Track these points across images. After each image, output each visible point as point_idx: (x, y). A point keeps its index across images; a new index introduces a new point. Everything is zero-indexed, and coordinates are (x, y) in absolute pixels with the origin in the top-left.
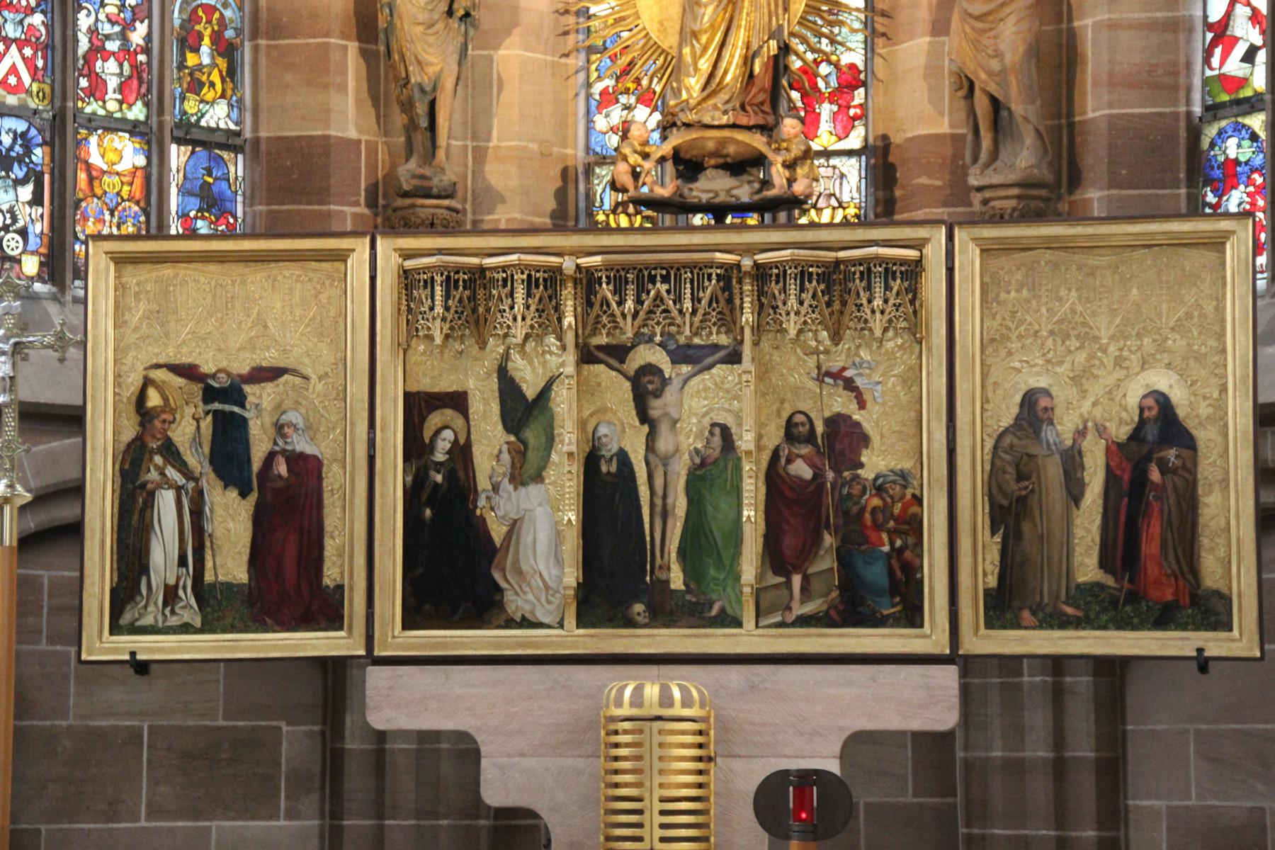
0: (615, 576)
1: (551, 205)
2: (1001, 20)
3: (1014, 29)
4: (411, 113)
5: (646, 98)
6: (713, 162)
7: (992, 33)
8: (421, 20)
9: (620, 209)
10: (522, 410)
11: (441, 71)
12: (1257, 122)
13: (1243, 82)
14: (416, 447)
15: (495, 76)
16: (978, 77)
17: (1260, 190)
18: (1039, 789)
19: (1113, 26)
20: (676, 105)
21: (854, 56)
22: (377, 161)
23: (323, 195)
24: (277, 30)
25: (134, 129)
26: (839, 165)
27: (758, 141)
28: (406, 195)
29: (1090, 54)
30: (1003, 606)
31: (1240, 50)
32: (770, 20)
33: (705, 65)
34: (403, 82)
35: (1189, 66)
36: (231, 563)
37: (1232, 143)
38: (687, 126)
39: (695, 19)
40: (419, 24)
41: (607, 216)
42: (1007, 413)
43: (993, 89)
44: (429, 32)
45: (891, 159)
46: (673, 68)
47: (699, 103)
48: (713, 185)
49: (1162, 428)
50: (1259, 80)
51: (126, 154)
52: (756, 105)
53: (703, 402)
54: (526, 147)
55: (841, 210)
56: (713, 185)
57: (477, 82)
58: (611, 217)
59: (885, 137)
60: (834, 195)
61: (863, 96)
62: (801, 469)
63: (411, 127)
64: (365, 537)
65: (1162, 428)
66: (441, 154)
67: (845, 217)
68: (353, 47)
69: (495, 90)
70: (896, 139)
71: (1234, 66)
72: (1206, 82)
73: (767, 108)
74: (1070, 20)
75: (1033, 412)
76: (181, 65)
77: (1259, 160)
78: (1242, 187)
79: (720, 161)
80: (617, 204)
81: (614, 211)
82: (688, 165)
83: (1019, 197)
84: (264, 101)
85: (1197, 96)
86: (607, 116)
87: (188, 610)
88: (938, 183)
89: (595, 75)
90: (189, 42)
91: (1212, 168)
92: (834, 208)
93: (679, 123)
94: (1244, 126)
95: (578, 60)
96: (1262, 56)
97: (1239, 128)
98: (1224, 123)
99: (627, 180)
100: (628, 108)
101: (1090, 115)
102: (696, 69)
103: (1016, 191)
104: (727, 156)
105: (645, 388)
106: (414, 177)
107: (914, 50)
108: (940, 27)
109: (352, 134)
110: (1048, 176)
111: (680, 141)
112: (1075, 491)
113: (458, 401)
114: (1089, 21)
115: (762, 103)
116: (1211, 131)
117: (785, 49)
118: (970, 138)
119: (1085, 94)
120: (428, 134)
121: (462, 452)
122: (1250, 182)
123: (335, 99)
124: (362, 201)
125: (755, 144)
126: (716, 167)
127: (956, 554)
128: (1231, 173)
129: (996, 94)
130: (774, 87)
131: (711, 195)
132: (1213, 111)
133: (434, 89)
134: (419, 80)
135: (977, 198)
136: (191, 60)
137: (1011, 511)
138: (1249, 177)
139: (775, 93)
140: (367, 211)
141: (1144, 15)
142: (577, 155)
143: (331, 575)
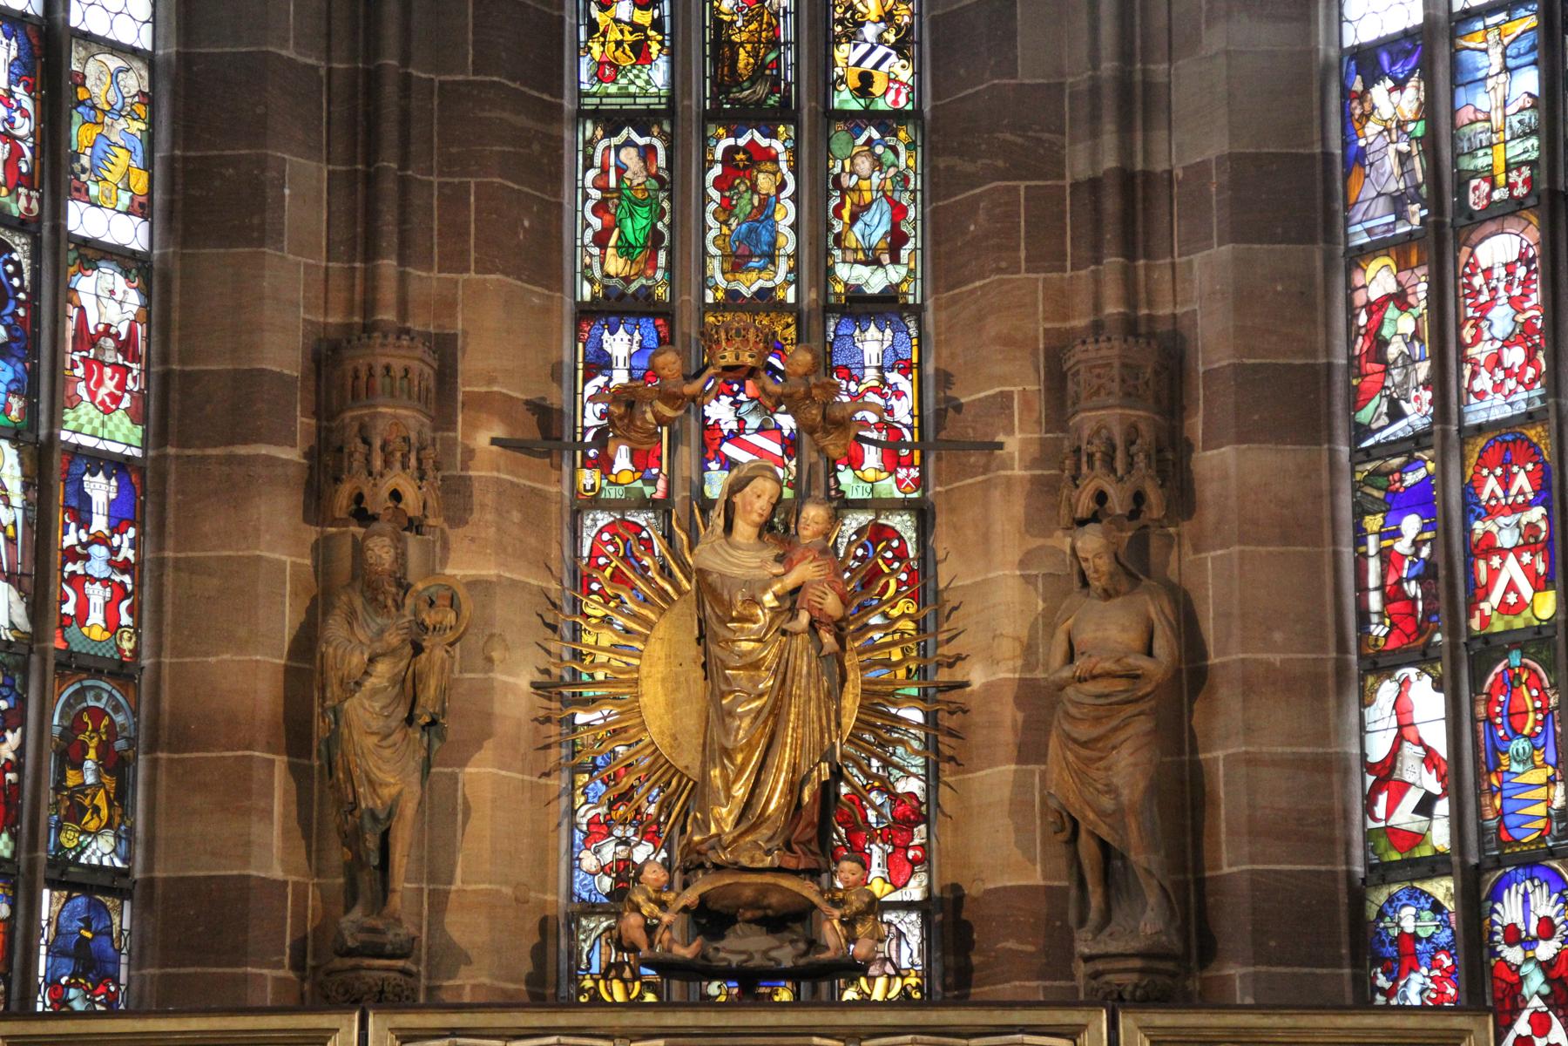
1: (527, 967)
2: (1114, 748)
3: (1132, 760)
4: (357, 849)
5: (649, 832)
6: (749, 915)
7: (1102, 764)
8: (374, 729)
9: (613, 973)
11: (400, 793)
12: (1441, 888)
13: (1418, 838)
15: (460, 801)
16: (1085, 817)
17: (1449, 974)
19: (1251, 761)
20: (702, 842)
21: (914, 786)
22: (306, 908)
23: (238, 955)
24: (183, 739)
26: (896, 921)
27: (808, 890)
28: (350, 953)
29: (1222, 794)
31: (1412, 798)
32: (822, 737)
33: (739, 791)
34: (347, 807)
35: (1346, 815)
37: (1408, 913)
38: (718, 867)
39: (727, 733)
40: (373, 733)
41: (596, 982)
43: (1104, 831)
44: (384, 744)
45: (964, 916)
46: (699, 793)
47: (735, 840)
48: (746, 944)
50: (1440, 836)
52: (803, 843)
54: (498, 891)
55: (898, 980)
56: (746, 944)
57: (443, 811)
58: (602, 983)
59: (956, 888)
60: (890, 959)
61: (924, 834)
63: (353, 869)
66: (395, 901)
67: (904, 988)
68: (281, 761)
69: (460, 817)
70: (972, 890)
71: (1405, 817)
72: (1368, 835)
73: (814, 847)
74: (1194, 750)
76: (60, 786)
77: (1444, 937)
78: (1424, 970)
79: (759, 913)
80: (610, 966)
81: (605, 975)
82: (710, 919)
83: (1141, 971)
84: (162, 831)
85: (1358, 852)
86: (597, 852)
88: (1030, 948)
89: (582, 799)
90: (71, 756)
91: (1383, 943)
92: (889, 977)
93: (708, 865)
94: (1423, 893)
95: (559, 782)
96: (1442, 807)
97: (1416, 895)
98: (1395, 888)
99: (639, 937)
100: (623, 841)
101: (1226, 870)
102: (729, 797)
103: (1137, 963)
104: (770, 907)
106: (362, 929)
107: (994, 778)
108: (1030, 750)
109: (277, 873)
110: (1177, 946)
111: (709, 887)
114: (1220, 754)
115: (810, 841)
116: (1380, 897)
117: (838, 774)
118: (1073, 893)
119: (1218, 844)
120: (378, 874)
122: (1434, 964)
123: (257, 829)
124: (287, 961)
125: (805, 893)
126: (749, 922)
128: (1407, 953)
129: (1108, 839)
130: (823, 825)
131: (743, 957)
132: (1381, 873)
133: (390, 816)
134: (371, 804)
135: (1081, 969)
136: (72, 779)
138: (1433, 958)
139: (824, 829)
140: (291, 975)
141: (1288, 750)
142: (557, 900)
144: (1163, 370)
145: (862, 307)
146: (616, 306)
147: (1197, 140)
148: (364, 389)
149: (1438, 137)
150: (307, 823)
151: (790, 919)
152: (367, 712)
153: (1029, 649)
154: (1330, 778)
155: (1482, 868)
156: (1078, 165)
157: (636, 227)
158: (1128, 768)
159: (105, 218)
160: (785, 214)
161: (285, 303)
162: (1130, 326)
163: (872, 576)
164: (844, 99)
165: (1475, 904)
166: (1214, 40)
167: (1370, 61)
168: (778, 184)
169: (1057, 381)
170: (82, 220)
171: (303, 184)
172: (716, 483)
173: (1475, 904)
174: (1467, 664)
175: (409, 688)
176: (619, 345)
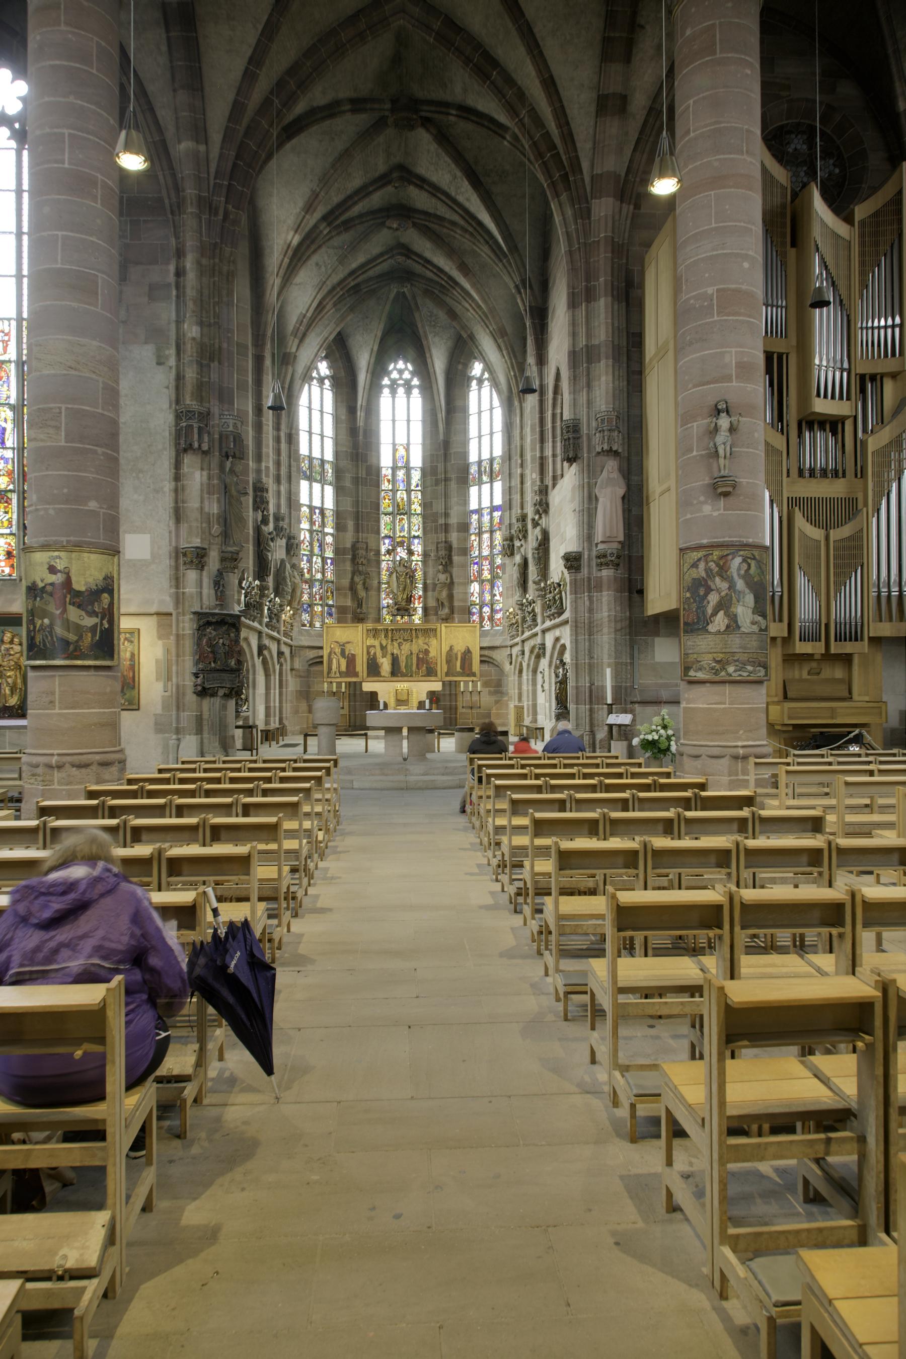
0: (395, 672)
10: (383, 648)
14: (368, 653)
18: (448, 698)
25: (321, 605)
30: (447, 674)
36: (343, 668)
42: (448, 649)
49: (468, 652)
50: (478, 602)
51: (320, 609)
53: (406, 647)
57: (367, 597)
62: (421, 656)
64: (361, 666)
65: (468, 652)
71: (474, 599)
75: (451, 648)
87: (338, 675)
105: (400, 645)
112: (457, 659)
113: (374, 646)
121: (375, 653)
127: (442, 668)
128: (474, 614)
137: (448, 662)
143: (357, 670)
144: (449, 548)
145: (415, 537)
146: (386, 537)
148: (358, 549)
149: (479, 521)
150: (353, 600)
151: (407, 610)
152: (360, 587)
153: (434, 579)
154: (467, 594)
156: (440, 522)
157: (389, 527)
158: (444, 594)
159: (329, 530)
160: (406, 526)
161: (349, 539)
162: (446, 542)
163: (416, 570)
164: (413, 512)
165: (481, 608)
166: (455, 508)
168: (405, 522)
169: (437, 548)
171: (350, 524)
172: (398, 558)
173: (481, 608)
174: (482, 582)
175: (364, 584)
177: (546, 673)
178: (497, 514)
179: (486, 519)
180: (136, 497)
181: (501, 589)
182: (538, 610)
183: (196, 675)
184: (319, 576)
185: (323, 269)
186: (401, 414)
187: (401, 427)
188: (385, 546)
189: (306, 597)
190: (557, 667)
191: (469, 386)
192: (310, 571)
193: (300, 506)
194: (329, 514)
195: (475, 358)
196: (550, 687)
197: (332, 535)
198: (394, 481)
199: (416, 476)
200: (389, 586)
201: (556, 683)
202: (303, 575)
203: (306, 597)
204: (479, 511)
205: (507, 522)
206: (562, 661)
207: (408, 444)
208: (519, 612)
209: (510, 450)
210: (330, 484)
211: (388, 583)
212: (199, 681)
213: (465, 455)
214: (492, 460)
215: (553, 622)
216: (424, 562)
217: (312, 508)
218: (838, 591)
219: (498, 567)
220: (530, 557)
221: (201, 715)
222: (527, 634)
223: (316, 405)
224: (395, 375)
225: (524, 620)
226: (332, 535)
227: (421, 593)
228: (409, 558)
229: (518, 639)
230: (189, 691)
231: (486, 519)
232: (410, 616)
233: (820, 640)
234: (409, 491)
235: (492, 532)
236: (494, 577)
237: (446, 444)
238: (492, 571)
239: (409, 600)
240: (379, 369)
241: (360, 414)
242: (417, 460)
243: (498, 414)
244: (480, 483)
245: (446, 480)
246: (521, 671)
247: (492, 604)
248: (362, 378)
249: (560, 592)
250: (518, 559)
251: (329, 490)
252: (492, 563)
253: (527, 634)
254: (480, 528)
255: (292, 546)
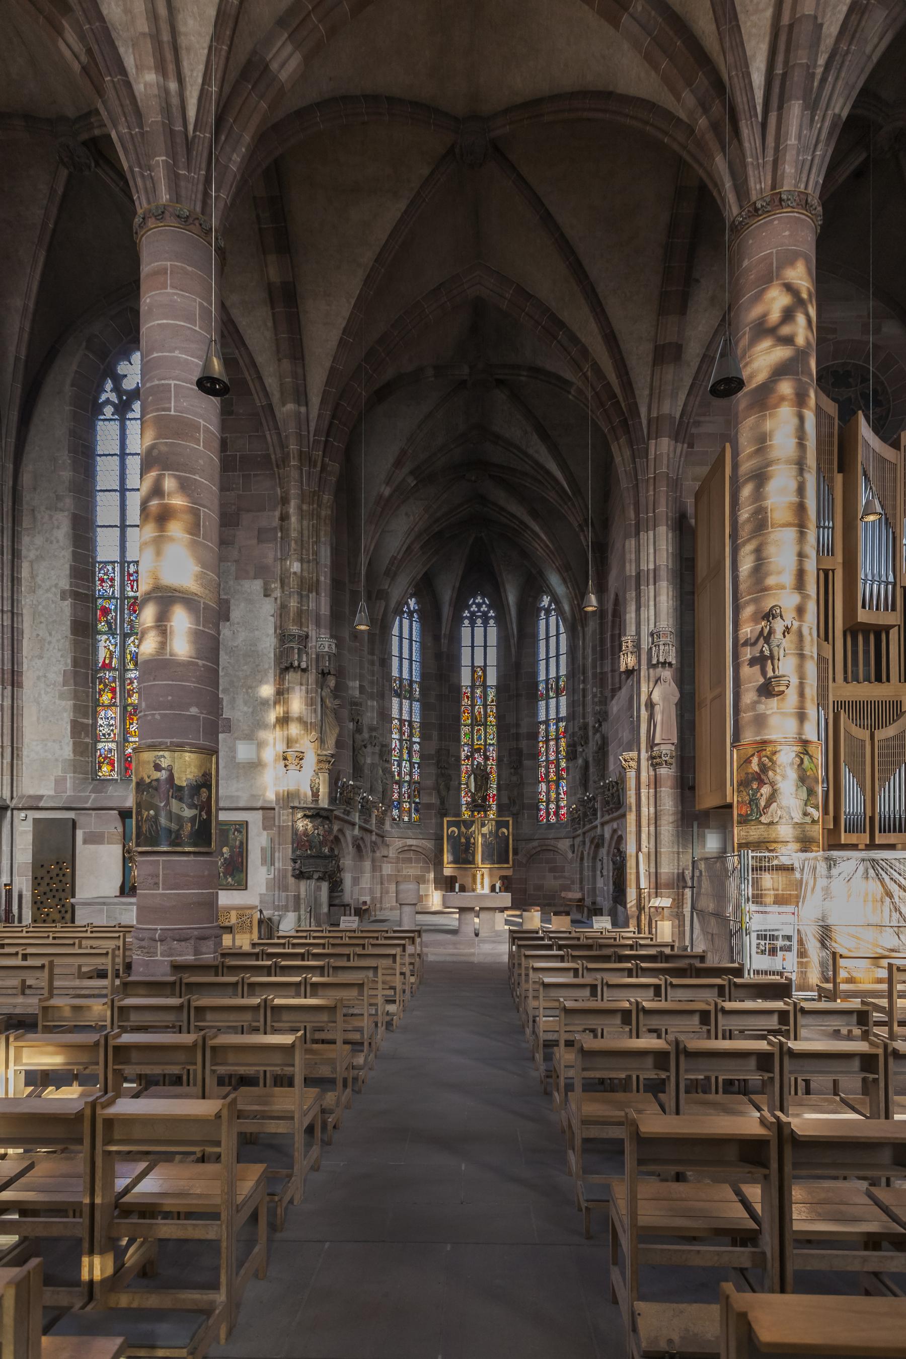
25: (409, 803)
144: (519, 752)
145: (490, 745)
147: (524, 730)
149: (547, 731)
155: (548, 802)
159: (416, 739)
163: (491, 772)
165: (548, 805)
167: (540, 723)
170: (414, 739)
171: (435, 734)
172: (476, 763)
173: (548, 805)
174: (548, 782)
176: (466, 749)
177: (605, 861)
178: (562, 724)
179: (553, 728)
180: (245, 709)
181: (565, 789)
182: (598, 805)
183: (294, 861)
184: (407, 778)
185: (412, 518)
186: (479, 641)
187: (479, 652)
188: (465, 751)
189: (396, 796)
190: (614, 855)
191: (538, 616)
192: (399, 774)
193: (391, 719)
194: (416, 725)
195: (544, 592)
196: (608, 872)
197: (418, 743)
198: (473, 698)
199: (491, 694)
200: (468, 787)
201: (614, 870)
202: (393, 776)
203: (396, 796)
204: (547, 722)
205: (570, 731)
206: (619, 850)
207: (485, 666)
208: (581, 808)
209: (573, 669)
210: (417, 701)
211: (467, 784)
212: (297, 866)
213: (535, 674)
214: (558, 678)
215: (611, 816)
216: (498, 766)
217: (400, 720)
218: (882, 786)
219: (563, 770)
220: (591, 759)
221: (299, 895)
222: (588, 827)
223: (406, 634)
224: (474, 608)
225: (585, 815)
226: (418, 743)
227: (495, 792)
228: (485, 762)
229: (580, 832)
230: (290, 873)
231: (553, 728)
232: (485, 811)
233: (865, 832)
234: (485, 706)
235: (557, 739)
236: (559, 778)
237: (518, 666)
238: (557, 773)
239: (485, 798)
240: (460, 604)
241: (444, 641)
242: (492, 680)
243: (563, 638)
244: (548, 698)
245: (518, 696)
246: (582, 859)
247: (558, 800)
248: (446, 611)
249: (618, 790)
250: (580, 761)
251: (416, 705)
252: (558, 766)
253: (588, 827)
254: (547, 736)
255: (385, 752)
